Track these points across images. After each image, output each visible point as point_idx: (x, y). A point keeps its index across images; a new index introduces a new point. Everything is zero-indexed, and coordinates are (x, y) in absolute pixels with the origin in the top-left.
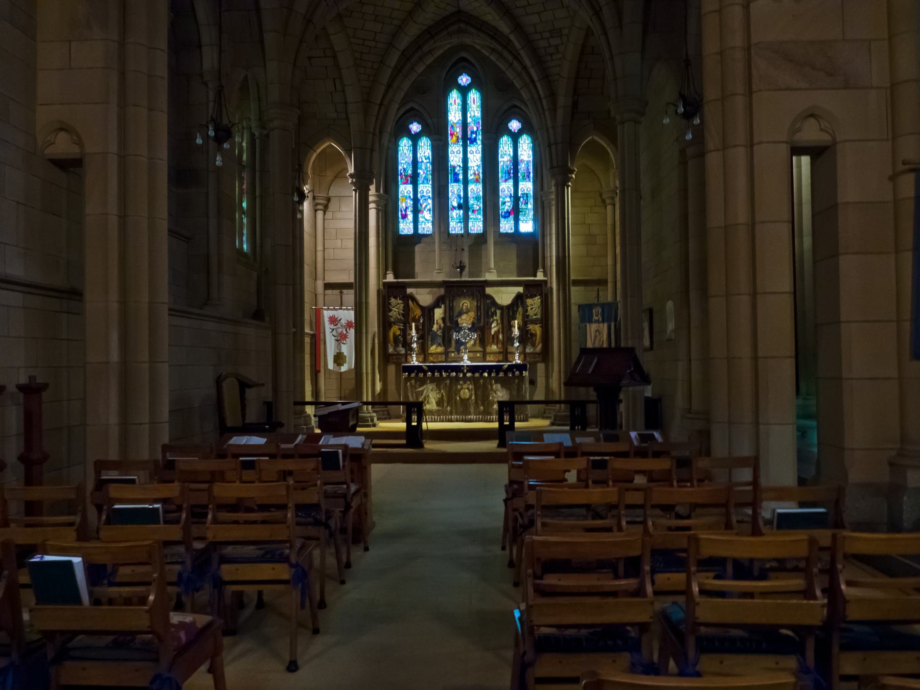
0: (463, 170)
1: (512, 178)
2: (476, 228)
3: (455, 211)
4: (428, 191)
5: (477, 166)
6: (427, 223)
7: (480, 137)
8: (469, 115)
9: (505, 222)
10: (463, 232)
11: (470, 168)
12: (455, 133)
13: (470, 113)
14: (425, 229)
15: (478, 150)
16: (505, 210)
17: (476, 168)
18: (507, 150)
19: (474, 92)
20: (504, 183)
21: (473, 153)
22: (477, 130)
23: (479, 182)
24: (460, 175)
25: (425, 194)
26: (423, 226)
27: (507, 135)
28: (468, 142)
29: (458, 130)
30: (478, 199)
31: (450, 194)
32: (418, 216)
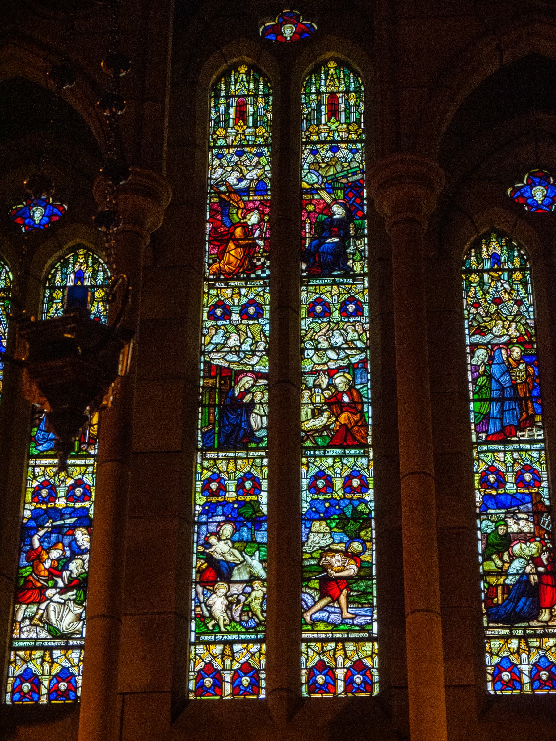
0: (269, 388)
1: (538, 418)
2: (340, 674)
3: (222, 588)
4: (78, 492)
5: (351, 368)
6: (56, 653)
7: (363, 244)
8: (308, 158)
9: (514, 643)
10: (262, 697)
11: (310, 380)
12: (238, 232)
13: (314, 152)
14: (46, 683)
15: (352, 300)
16: (510, 581)
17: (340, 380)
18: (506, 296)
19: (332, 71)
20: (501, 447)
21: (327, 312)
22: (350, 216)
23: (364, 446)
24: (258, 409)
25: (61, 503)
26: (35, 667)
27: (501, 235)
28: (304, 266)
29: (253, 218)
30: (352, 526)
31: (200, 499)
32: (15, 613)
